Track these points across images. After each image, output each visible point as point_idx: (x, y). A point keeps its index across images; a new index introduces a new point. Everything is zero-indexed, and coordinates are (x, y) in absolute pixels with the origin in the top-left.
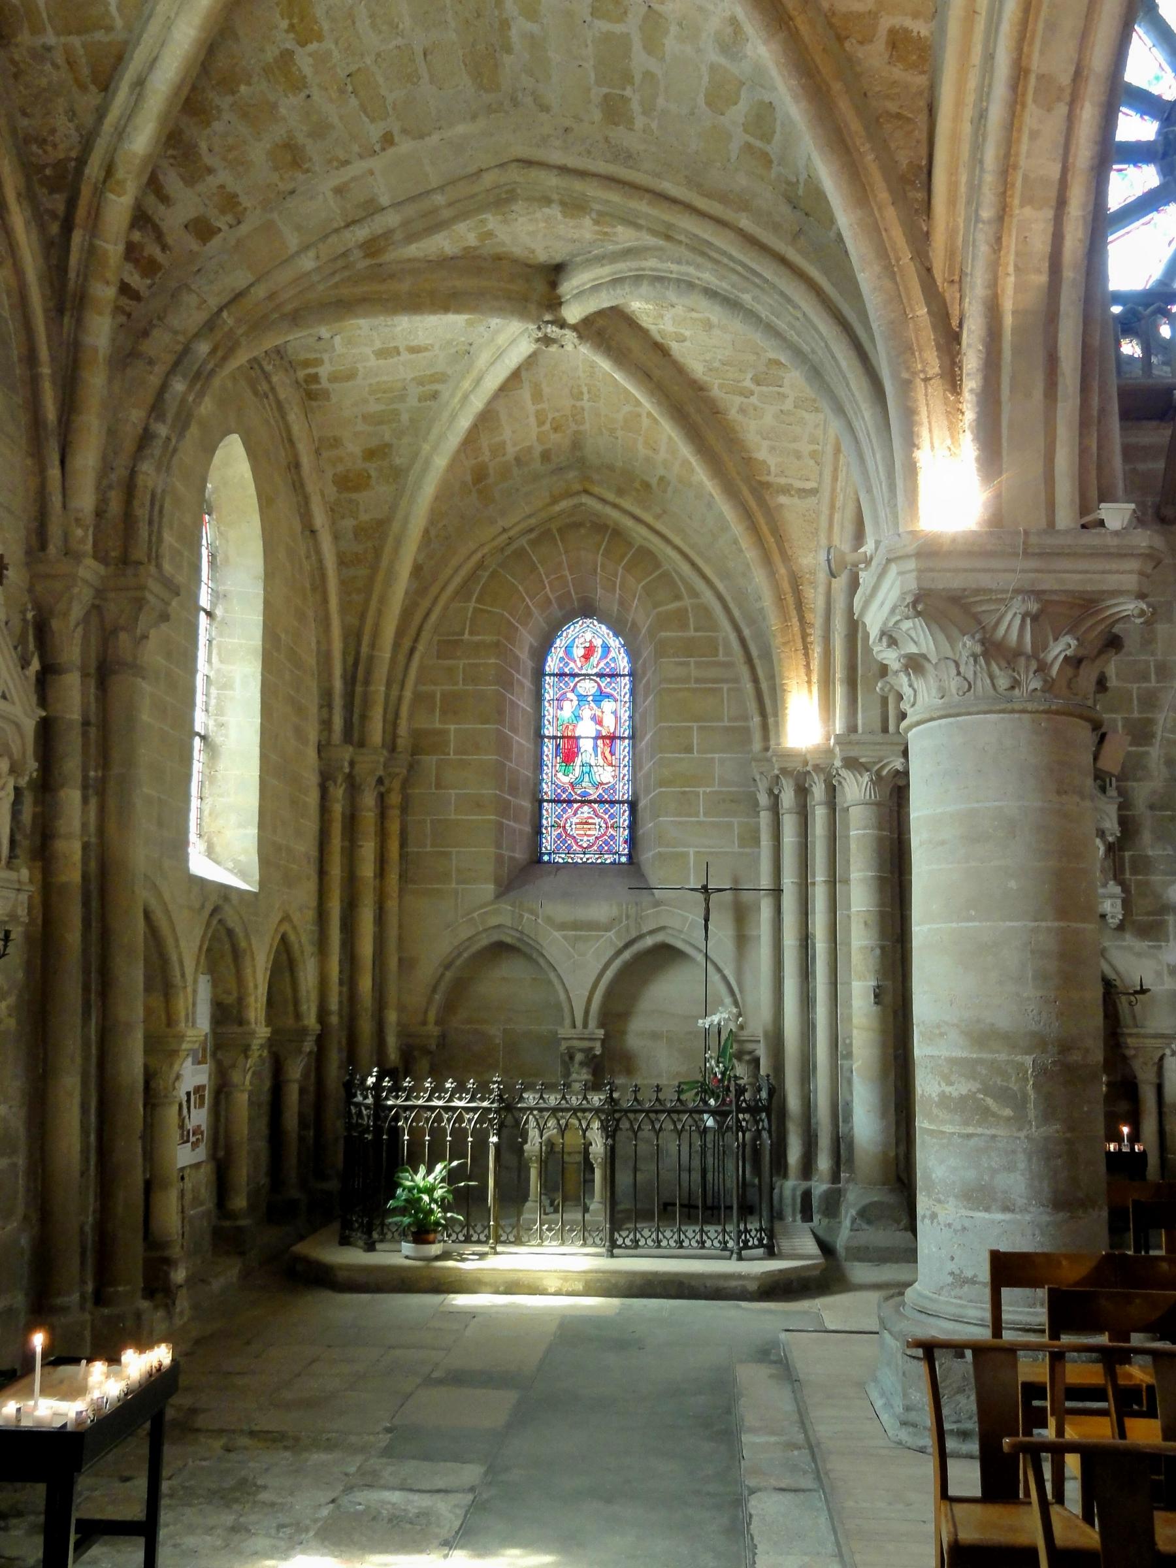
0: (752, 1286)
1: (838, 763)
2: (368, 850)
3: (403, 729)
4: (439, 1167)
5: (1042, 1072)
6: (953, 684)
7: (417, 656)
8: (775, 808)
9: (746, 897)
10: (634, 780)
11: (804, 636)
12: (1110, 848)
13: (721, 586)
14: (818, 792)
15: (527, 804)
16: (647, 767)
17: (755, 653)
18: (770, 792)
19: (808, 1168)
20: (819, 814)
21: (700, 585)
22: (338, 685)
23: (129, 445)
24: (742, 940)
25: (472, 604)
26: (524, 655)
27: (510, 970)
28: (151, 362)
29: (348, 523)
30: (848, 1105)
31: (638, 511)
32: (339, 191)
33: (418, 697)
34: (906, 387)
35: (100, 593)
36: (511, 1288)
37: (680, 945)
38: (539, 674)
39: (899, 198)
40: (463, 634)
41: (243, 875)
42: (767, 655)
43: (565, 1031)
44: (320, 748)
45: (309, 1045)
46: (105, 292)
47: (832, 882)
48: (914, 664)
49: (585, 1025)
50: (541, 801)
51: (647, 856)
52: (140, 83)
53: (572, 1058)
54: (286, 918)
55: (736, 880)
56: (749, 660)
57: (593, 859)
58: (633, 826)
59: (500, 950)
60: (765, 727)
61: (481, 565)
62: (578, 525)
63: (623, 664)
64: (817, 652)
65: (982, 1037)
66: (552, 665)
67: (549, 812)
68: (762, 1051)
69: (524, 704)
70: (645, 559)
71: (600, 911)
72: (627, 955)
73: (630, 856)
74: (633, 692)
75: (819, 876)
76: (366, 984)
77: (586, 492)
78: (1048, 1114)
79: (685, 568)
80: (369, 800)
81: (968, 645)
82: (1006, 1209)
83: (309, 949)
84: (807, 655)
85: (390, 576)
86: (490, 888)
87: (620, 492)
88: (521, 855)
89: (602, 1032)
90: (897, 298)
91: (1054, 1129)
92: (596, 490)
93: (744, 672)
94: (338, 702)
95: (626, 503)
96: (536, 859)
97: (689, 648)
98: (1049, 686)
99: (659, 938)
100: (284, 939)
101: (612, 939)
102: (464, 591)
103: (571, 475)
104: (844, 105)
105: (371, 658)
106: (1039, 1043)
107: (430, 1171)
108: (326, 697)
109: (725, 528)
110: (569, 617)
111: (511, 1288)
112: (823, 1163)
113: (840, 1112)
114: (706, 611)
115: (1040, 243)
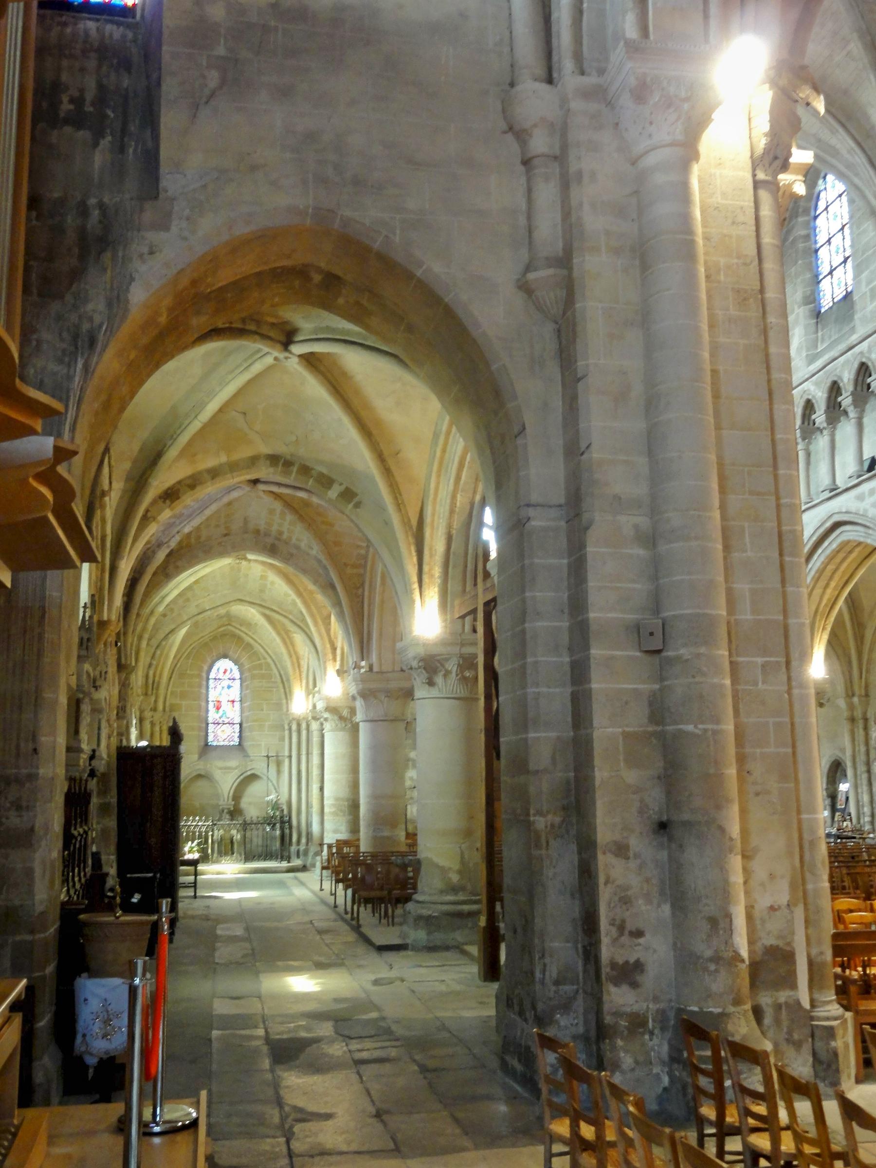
0: (284, 870)
1: (310, 718)
3: (168, 704)
4: (196, 842)
6: (334, 725)
7: (172, 679)
8: (290, 729)
9: (280, 758)
10: (241, 716)
11: (300, 675)
13: (274, 657)
14: (304, 726)
15: (204, 725)
16: (246, 714)
17: (284, 679)
18: (289, 724)
19: (299, 842)
20: (304, 733)
21: (267, 656)
23: (147, 666)
24: (279, 772)
25: (190, 661)
26: (204, 675)
27: (201, 783)
28: (152, 647)
30: (311, 822)
31: (247, 632)
32: (197, 606)
33: (172, 693)
34: (325, 662)
35: (141, 703)
36: (218, 873)
37: (258, 773)
38: (208, 679)
39: (324, 622)
40: (187, 670)
42: (288, 680)
43: (221, 803)
46: (146, 636)
47: (308, 754)
48: (326, 719)
49: (228, 800)
50: (208, 724)
51: (247, 744)
52: (163, 598)
53: (223, 811)
55: (277, 753)
56: (283, 682)
57: (226, 743)
58: (240, 732)
59: (199, 776)
60: (287, 703)
61: (193, 648)
62: (225, 635)
63: (237, 675)
64: (304, 682)
65: (337, 799)
66: (212, 675)
67: (211, 728)
68: (285, 808)
69: (204, 691)
70: (249, 646)
71: (233, 763)
72: (242, 777)
73: (239, 742)
74: (241, 685)
75: (304, 752)
77: (229, 624)
78: (350, 814)
79: (262, 650)
80: (157, 729)
81: (336, 718)
82: (341, 833)
84: (301, 682)
85: (167, 656)
86: (196, 756)
87: (241, 625)
88: (202, 743)
89: (233, 803)
90: (323, 644)
91: (351, 817)
92: (234, 624)
93: (281, 685)
95: (243, 629)
96: (206, 745)
97: (263, 676)
99: (252, 772)
101: (237, 773)
102: (188, 657)
103: (225, 619)
104: (313, 607)
105: (159, 683)
106: (348, 800)
107: (192, 843)
109: (275, 640)
110: (218, 659)
111: (218, 873)
112: (304, 840)
113: (309, 825)
114: (268, 665)
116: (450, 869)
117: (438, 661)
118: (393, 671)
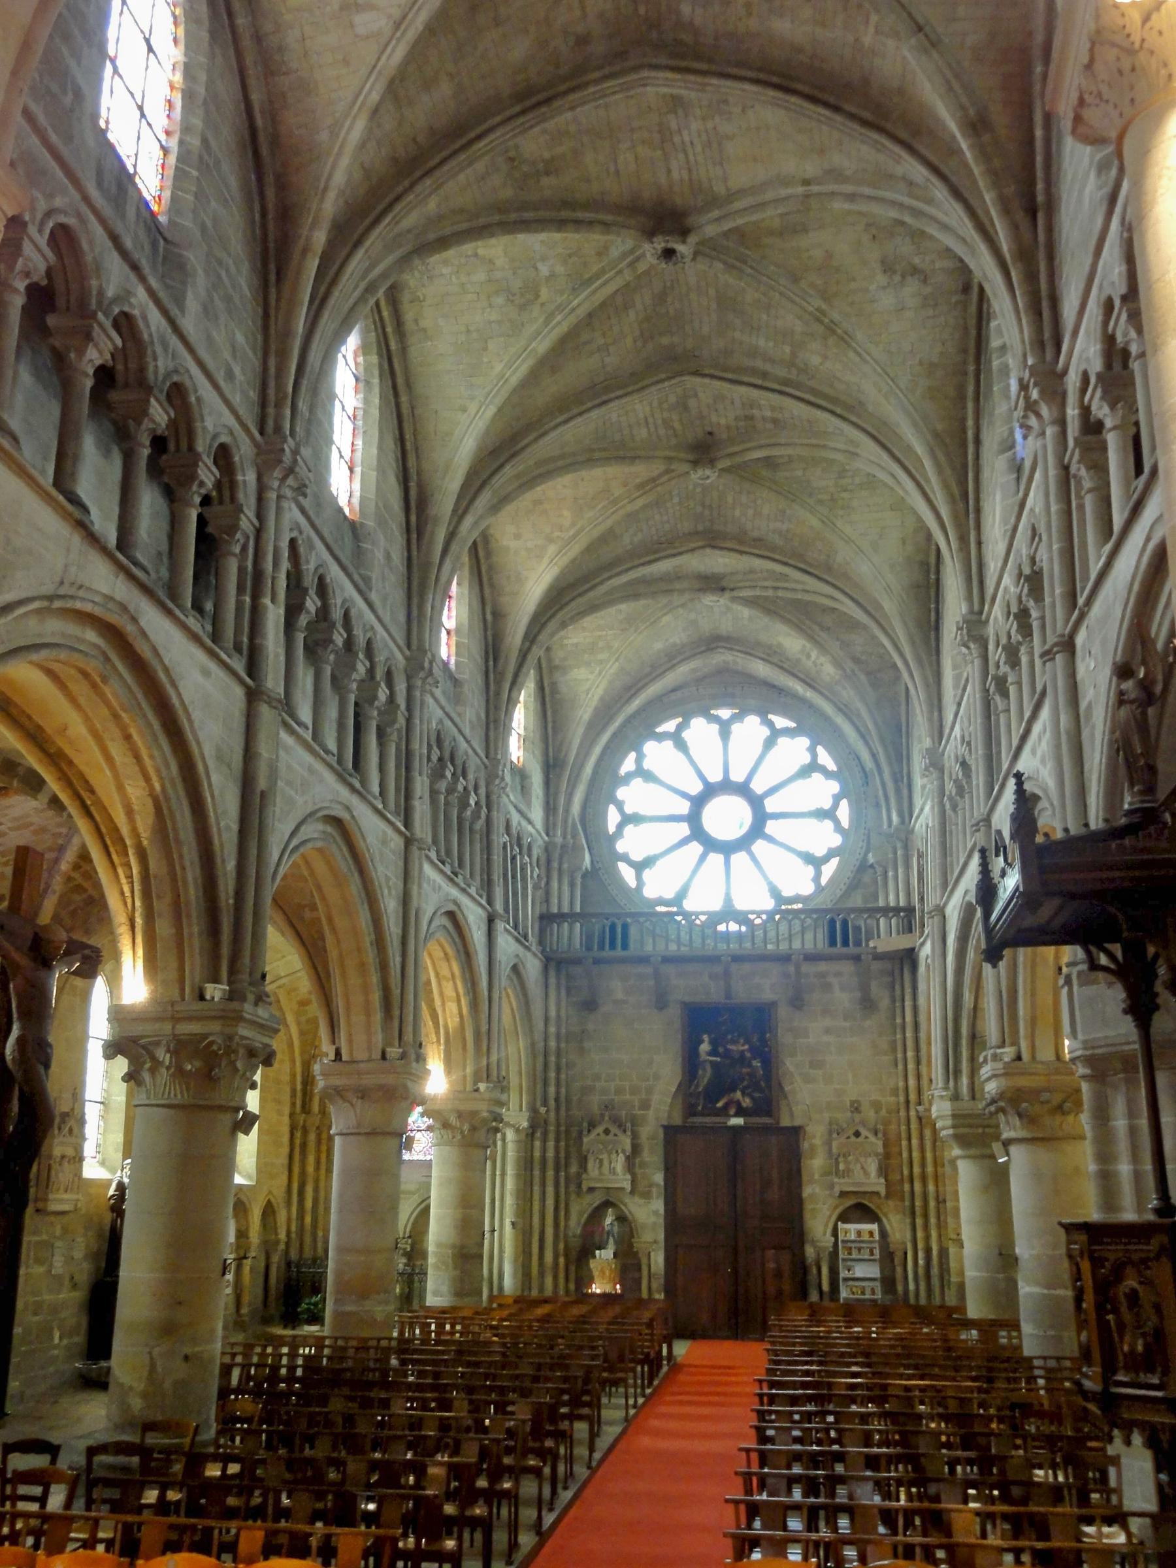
2: (311, 1159)
5: (454, 1255)
12: (627, 1158)
22: (299, 1087)
29: (303, 1019)
41: (248, 1177)
44: (292, 1115)
45: (282, 1246)
54: (270, 1192)
76: (308, 1219)
78: (455, 1268)
80: (312, 1137)
83: (282, 1205)
91: (458, 1272)
94: (299, 1094)
98: (463, 1137)
100: (269, 1202)
106: (454, 1246)
108: (294, 1091)
115: (455, 1010)
116: (131, 1388)
117: (143, 1047)
118: (369, 1060)
